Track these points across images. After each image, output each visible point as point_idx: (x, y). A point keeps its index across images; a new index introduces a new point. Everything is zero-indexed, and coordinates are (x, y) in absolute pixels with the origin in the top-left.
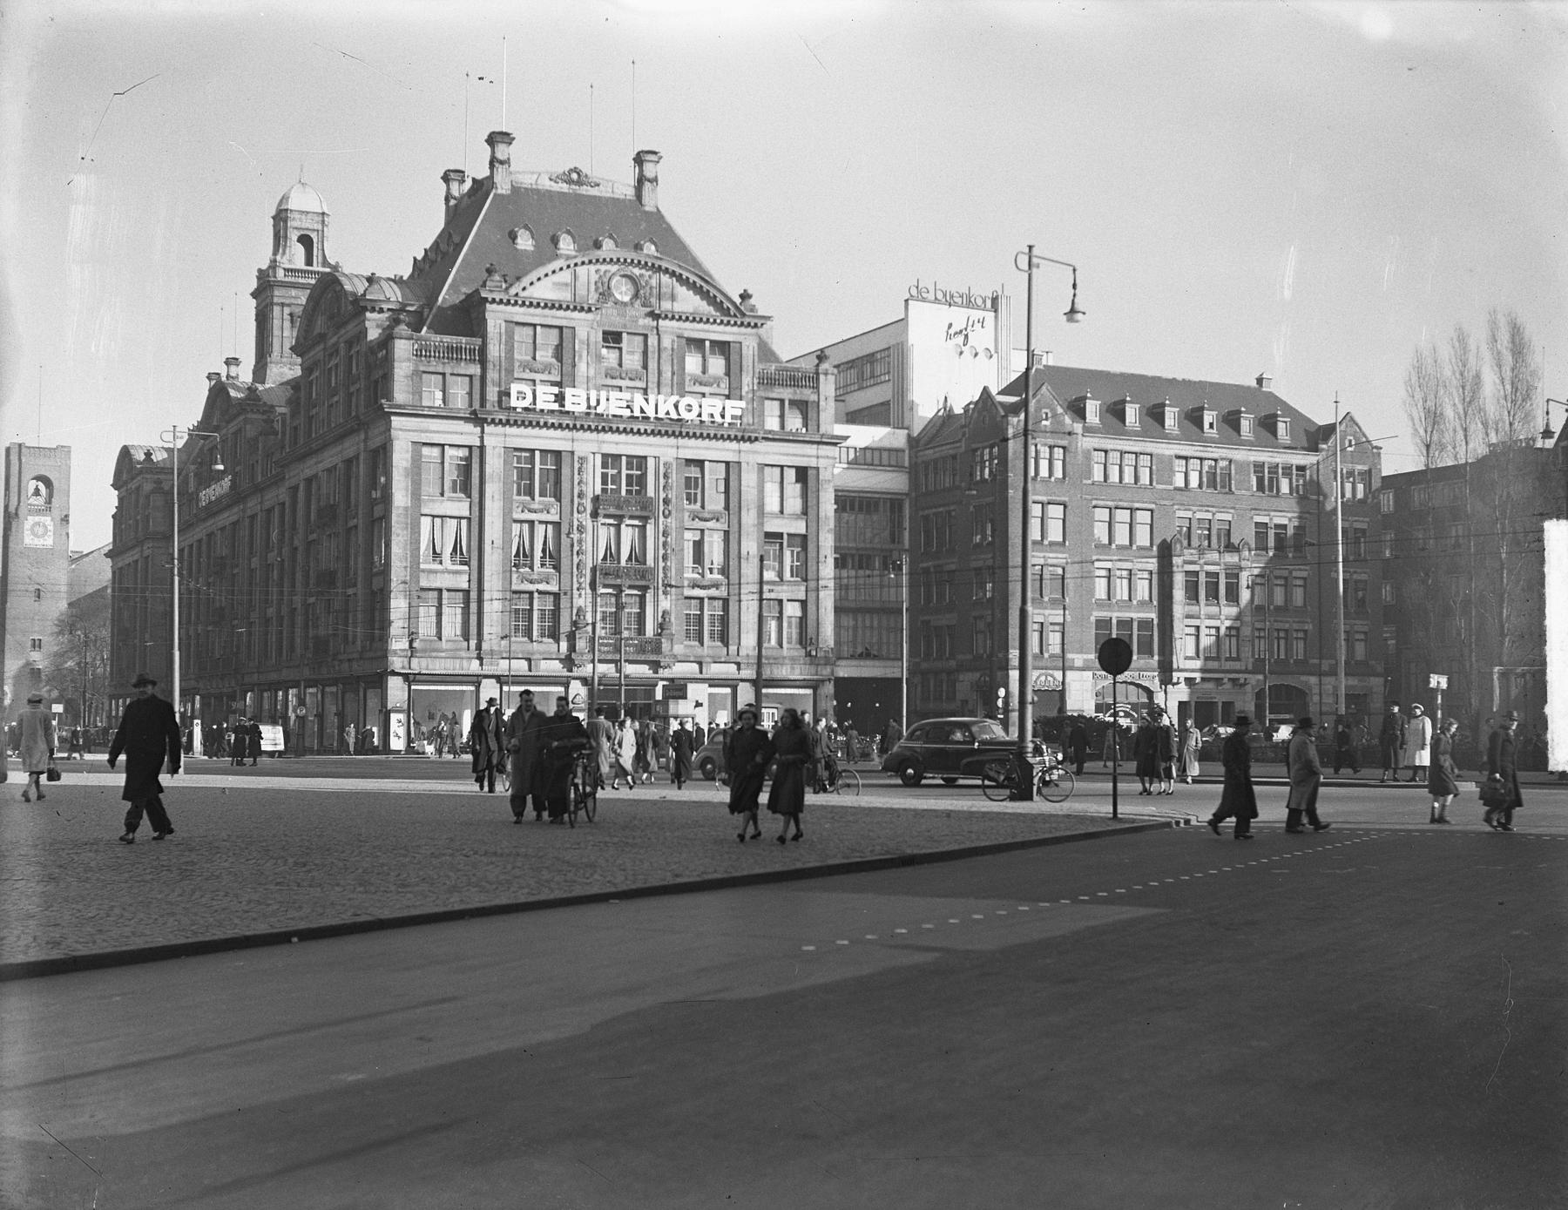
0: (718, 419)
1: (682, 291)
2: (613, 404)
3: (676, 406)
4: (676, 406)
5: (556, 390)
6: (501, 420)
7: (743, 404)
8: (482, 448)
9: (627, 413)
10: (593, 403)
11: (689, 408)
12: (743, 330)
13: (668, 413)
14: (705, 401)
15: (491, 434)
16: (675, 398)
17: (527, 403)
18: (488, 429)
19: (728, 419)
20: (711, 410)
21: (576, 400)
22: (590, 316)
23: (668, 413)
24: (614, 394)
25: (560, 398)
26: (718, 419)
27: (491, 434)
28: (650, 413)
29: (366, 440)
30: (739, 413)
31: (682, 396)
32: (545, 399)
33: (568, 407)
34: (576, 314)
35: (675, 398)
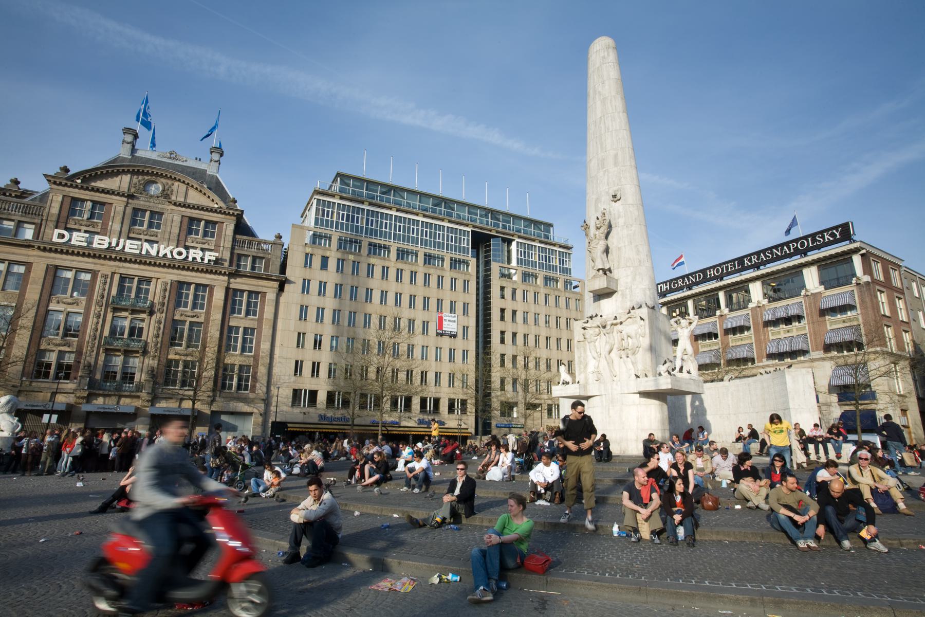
0: (199, 260)
2: (131, 247)
3: (172, 252)
4: (172, 252)
5: (87, 235)
6: (62, 250)
7: (217, 254)
9: (138, 252)
10: (114, 244)
11: (180, 254)
12: (228, 217)
13: (166, 254)
14: (191, 251)
16: (171, 248)
19: (206, 261)
20: (195, 256)
21: (100, 242)
22: (125, 199)
23: (166, 254)
24: (128, 242)
26: (199, 260)
28: (153, 252)
30: (214, 258)
31: (177, 247)
32: (78, 239)
33: (95, 245)
34: (113, 197)
35: (171, 248)
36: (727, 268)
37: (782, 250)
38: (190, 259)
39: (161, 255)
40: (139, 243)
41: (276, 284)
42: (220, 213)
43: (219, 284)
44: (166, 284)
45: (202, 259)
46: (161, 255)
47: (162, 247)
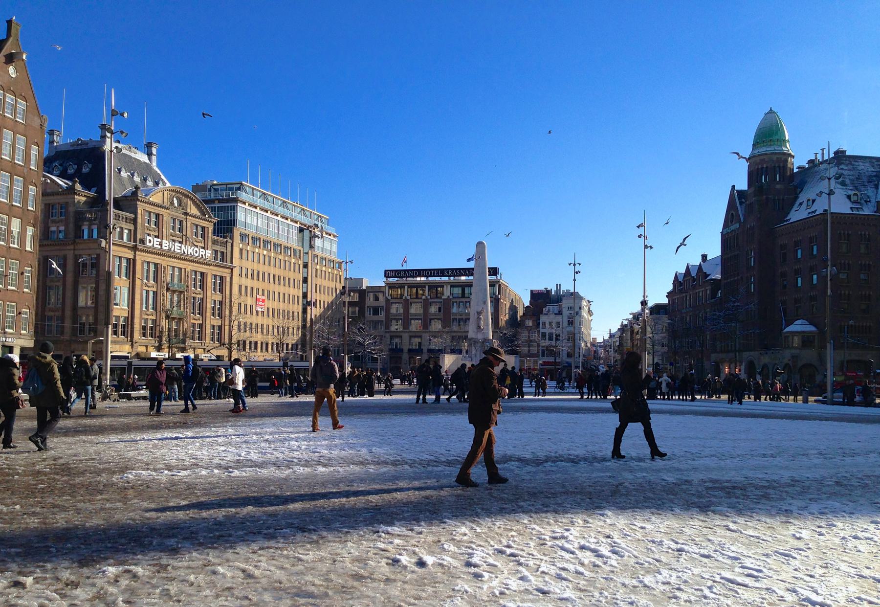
1: (193, 207)
8: (134, 260)
9: (180, 251)
14: (201, 250)
15: (139, 255)
17: (151, 244)
18: (137, 252)
21: (166, 245)
25: (161, 244)
27: (139, 255)
29: (74, 249)
33: (164, 247)
36: (434, 273)
37: (465, 271)
38: (201, 256)
39: (189, 253)
40: (180, 245)
41: (229, 271)
42: (208, 221)
43: (210, 271)
44: (188, 272)
45: (205, 255)
46: (189, 253)
47: (189, 247)
